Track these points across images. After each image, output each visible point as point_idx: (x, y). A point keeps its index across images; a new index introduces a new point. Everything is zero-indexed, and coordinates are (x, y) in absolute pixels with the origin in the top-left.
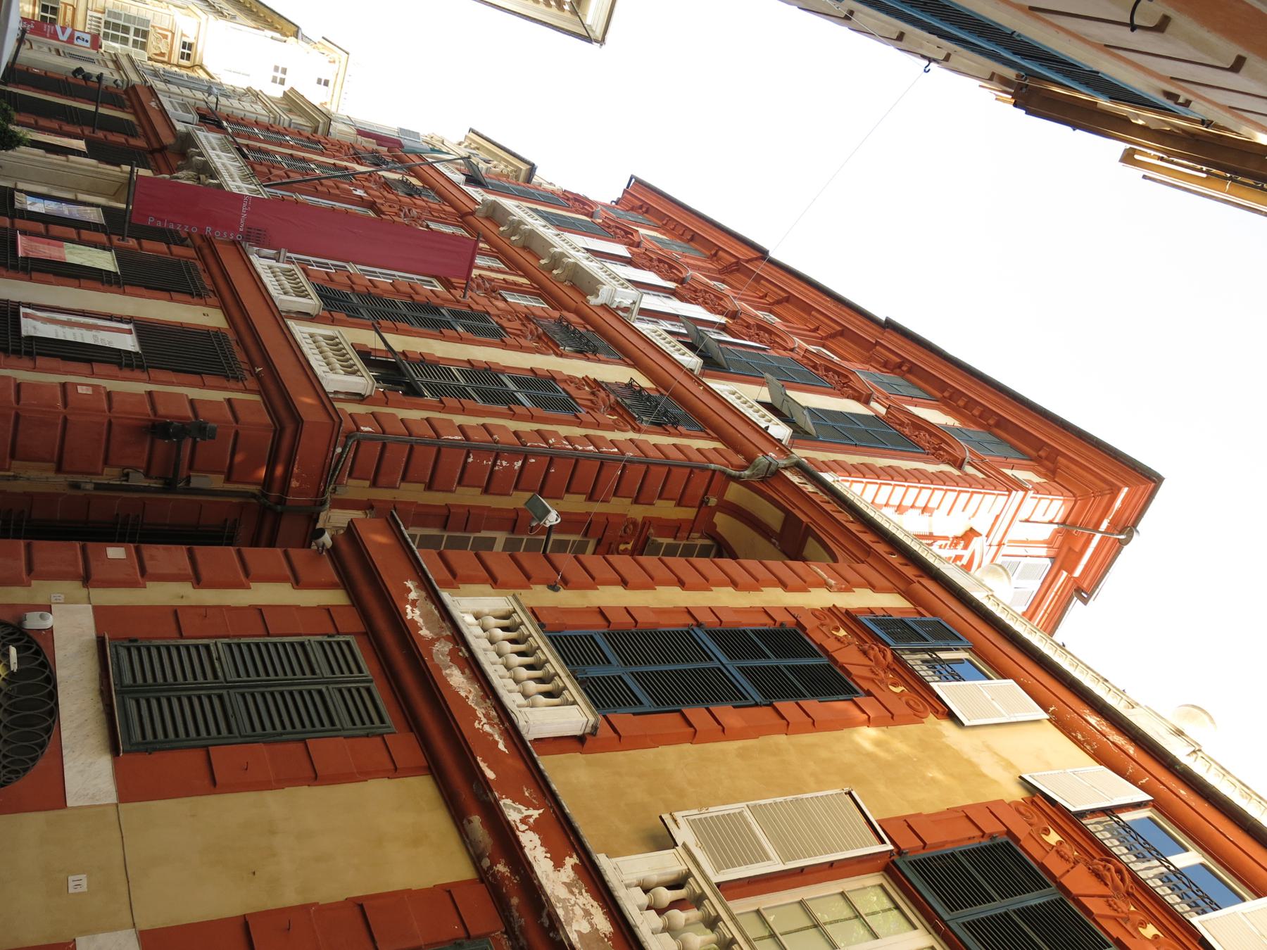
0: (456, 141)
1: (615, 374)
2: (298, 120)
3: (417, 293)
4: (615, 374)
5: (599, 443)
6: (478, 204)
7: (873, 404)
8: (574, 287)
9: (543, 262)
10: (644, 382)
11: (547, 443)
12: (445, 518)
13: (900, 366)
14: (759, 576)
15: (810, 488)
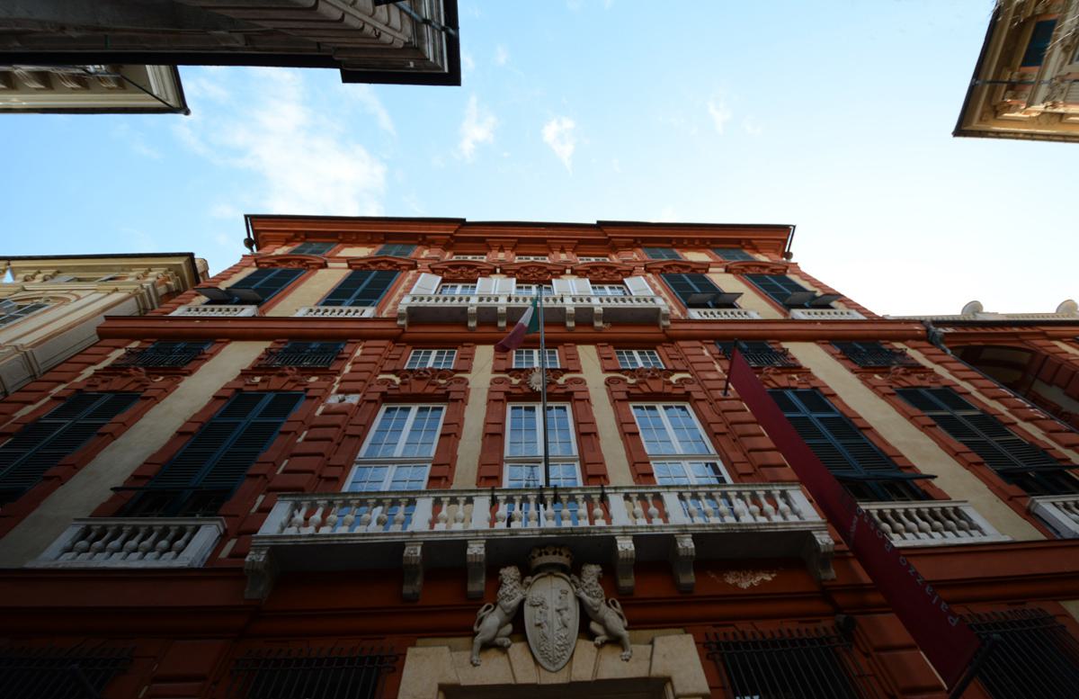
13: (635, 242)
15: (950, 330)
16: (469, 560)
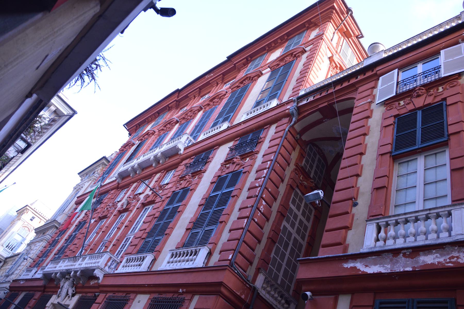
0: (80, 181)
1: (222, 153)
2: (50, 232)
3: (154, 215)
4: (222, 153)
5: (264, 167)
6: (115, 180)
7: (263, 72)
8: (170, 157)
10: (231, 144)
11: (257, 187)
12: (272, 241)
13: (247, 60)
14: (362, 125)
15: (311, 99)
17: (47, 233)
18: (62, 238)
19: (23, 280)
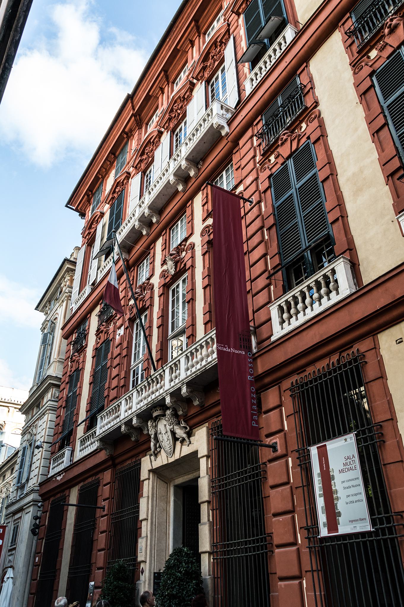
0: (44, 317)
2: (49, 396)
8: (204, 159)
9: (144, 232)
16: (135, 426)
17: (45, 400)
18: (81, 387)
19: (59, 474)
